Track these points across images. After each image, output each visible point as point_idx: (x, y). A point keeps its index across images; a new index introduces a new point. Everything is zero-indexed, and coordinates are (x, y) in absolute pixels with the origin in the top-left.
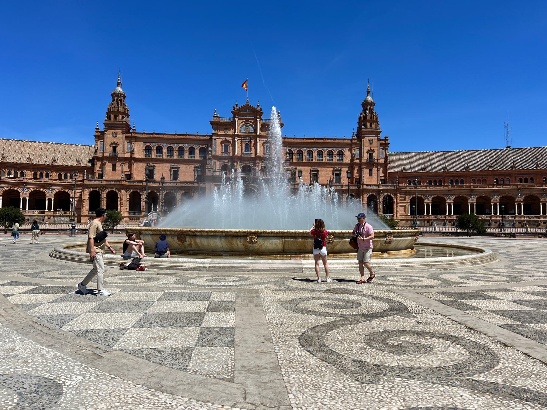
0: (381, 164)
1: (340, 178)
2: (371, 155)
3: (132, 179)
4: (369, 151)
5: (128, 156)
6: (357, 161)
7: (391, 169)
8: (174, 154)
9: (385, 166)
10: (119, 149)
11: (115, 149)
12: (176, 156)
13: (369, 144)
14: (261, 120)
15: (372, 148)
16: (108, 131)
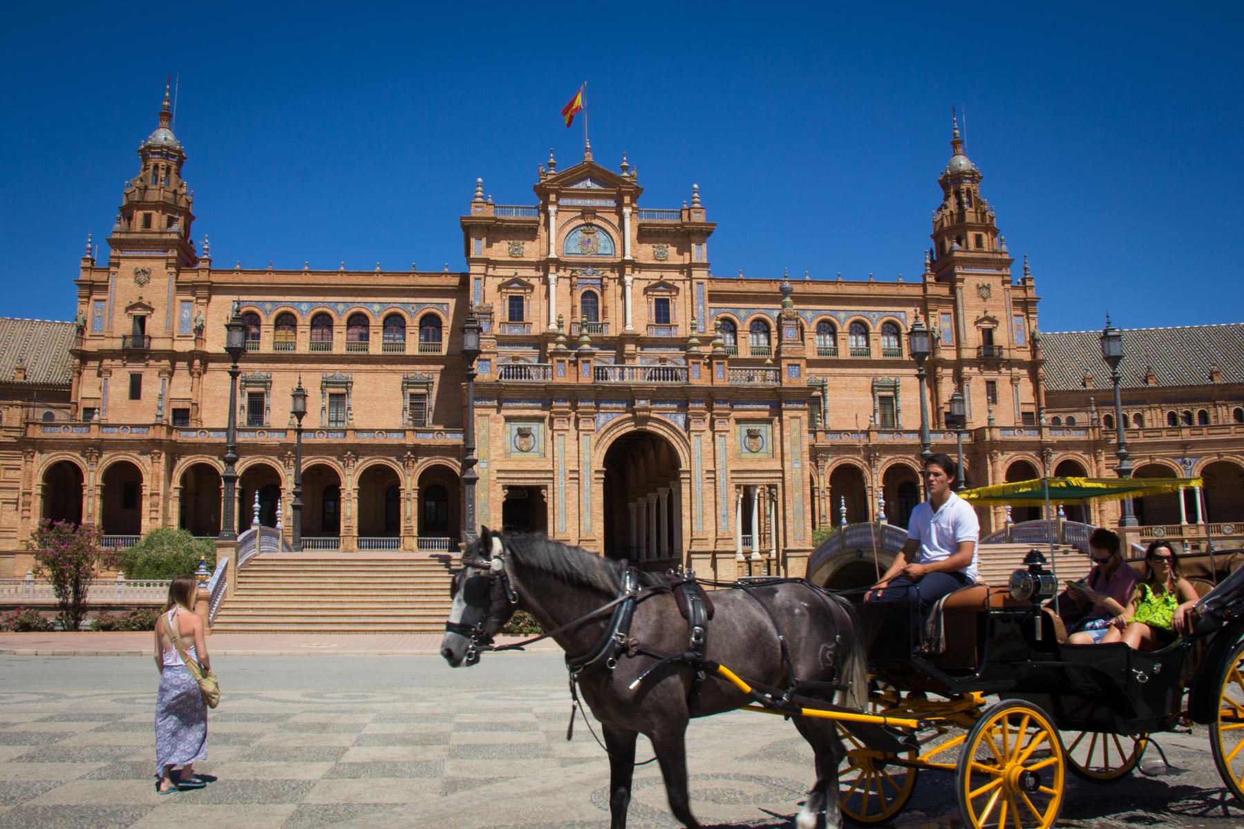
0: (1020, 364)
1: (895, 415)
2: (988, 335)
3: (193, 425)
4: (981, 321)
5: (186, 346)
6: (949, 355)
7: (1052, 381)
8: (336, 337)
9: (1033, 367)
10: (153, 325)
11: (141, 321)
12: (340, 342)
13: (979, 301)
14: (636, 212)
15: (990, 314)
16: (124, 263)
